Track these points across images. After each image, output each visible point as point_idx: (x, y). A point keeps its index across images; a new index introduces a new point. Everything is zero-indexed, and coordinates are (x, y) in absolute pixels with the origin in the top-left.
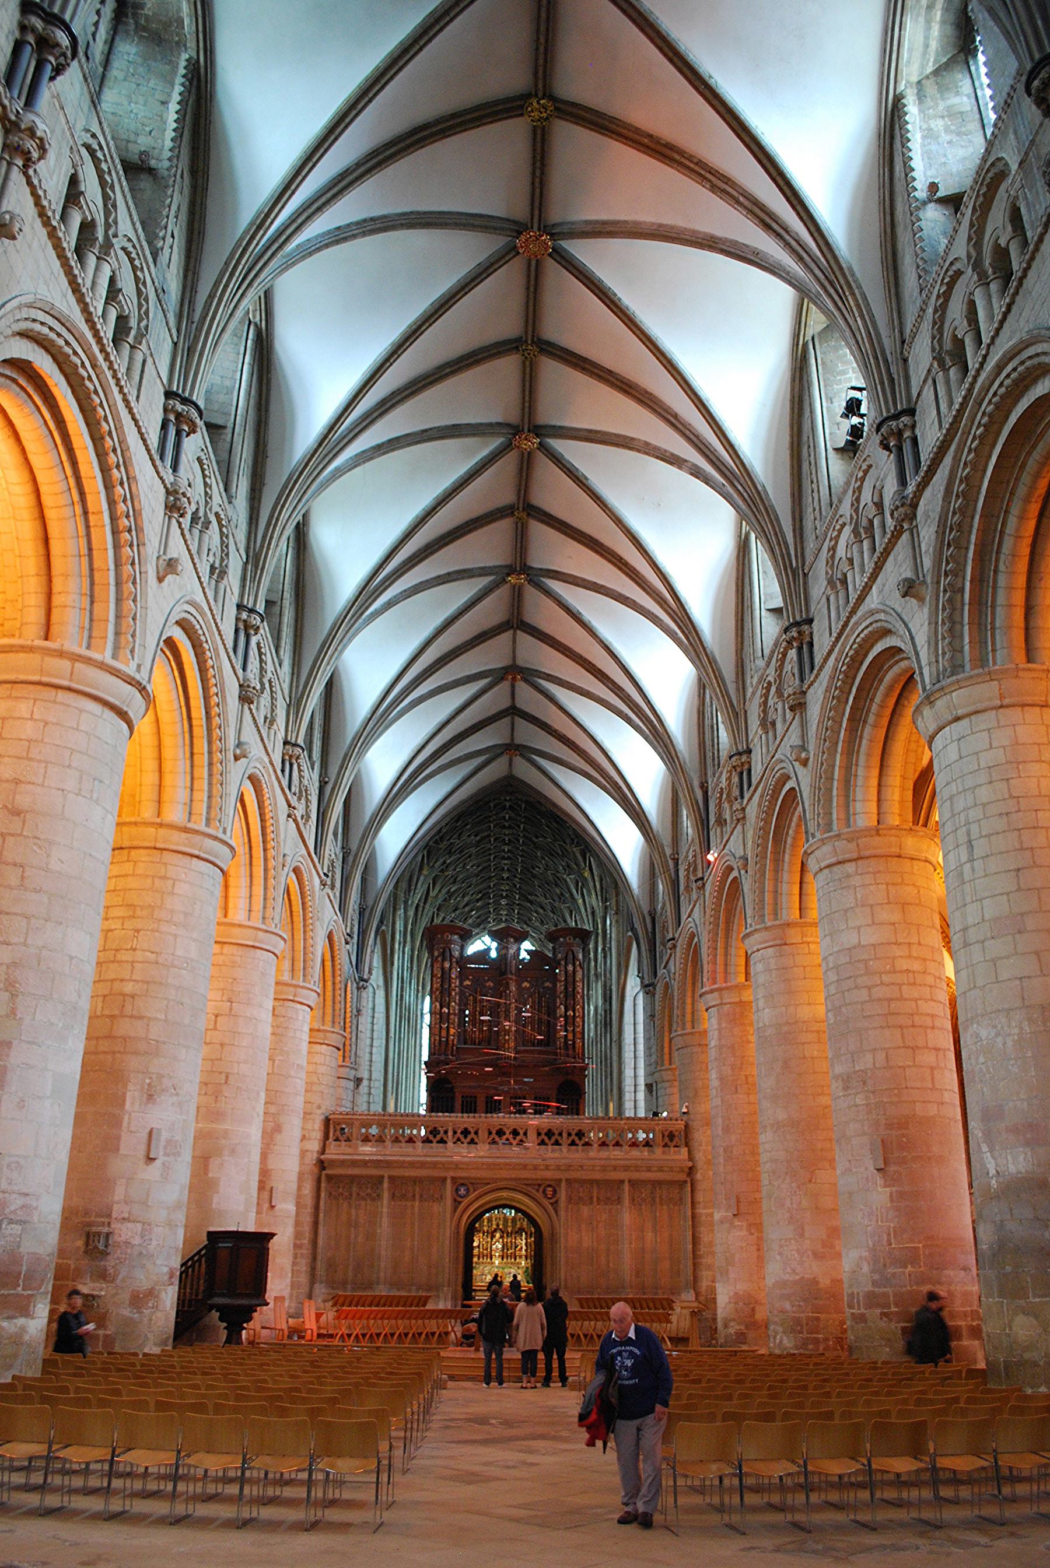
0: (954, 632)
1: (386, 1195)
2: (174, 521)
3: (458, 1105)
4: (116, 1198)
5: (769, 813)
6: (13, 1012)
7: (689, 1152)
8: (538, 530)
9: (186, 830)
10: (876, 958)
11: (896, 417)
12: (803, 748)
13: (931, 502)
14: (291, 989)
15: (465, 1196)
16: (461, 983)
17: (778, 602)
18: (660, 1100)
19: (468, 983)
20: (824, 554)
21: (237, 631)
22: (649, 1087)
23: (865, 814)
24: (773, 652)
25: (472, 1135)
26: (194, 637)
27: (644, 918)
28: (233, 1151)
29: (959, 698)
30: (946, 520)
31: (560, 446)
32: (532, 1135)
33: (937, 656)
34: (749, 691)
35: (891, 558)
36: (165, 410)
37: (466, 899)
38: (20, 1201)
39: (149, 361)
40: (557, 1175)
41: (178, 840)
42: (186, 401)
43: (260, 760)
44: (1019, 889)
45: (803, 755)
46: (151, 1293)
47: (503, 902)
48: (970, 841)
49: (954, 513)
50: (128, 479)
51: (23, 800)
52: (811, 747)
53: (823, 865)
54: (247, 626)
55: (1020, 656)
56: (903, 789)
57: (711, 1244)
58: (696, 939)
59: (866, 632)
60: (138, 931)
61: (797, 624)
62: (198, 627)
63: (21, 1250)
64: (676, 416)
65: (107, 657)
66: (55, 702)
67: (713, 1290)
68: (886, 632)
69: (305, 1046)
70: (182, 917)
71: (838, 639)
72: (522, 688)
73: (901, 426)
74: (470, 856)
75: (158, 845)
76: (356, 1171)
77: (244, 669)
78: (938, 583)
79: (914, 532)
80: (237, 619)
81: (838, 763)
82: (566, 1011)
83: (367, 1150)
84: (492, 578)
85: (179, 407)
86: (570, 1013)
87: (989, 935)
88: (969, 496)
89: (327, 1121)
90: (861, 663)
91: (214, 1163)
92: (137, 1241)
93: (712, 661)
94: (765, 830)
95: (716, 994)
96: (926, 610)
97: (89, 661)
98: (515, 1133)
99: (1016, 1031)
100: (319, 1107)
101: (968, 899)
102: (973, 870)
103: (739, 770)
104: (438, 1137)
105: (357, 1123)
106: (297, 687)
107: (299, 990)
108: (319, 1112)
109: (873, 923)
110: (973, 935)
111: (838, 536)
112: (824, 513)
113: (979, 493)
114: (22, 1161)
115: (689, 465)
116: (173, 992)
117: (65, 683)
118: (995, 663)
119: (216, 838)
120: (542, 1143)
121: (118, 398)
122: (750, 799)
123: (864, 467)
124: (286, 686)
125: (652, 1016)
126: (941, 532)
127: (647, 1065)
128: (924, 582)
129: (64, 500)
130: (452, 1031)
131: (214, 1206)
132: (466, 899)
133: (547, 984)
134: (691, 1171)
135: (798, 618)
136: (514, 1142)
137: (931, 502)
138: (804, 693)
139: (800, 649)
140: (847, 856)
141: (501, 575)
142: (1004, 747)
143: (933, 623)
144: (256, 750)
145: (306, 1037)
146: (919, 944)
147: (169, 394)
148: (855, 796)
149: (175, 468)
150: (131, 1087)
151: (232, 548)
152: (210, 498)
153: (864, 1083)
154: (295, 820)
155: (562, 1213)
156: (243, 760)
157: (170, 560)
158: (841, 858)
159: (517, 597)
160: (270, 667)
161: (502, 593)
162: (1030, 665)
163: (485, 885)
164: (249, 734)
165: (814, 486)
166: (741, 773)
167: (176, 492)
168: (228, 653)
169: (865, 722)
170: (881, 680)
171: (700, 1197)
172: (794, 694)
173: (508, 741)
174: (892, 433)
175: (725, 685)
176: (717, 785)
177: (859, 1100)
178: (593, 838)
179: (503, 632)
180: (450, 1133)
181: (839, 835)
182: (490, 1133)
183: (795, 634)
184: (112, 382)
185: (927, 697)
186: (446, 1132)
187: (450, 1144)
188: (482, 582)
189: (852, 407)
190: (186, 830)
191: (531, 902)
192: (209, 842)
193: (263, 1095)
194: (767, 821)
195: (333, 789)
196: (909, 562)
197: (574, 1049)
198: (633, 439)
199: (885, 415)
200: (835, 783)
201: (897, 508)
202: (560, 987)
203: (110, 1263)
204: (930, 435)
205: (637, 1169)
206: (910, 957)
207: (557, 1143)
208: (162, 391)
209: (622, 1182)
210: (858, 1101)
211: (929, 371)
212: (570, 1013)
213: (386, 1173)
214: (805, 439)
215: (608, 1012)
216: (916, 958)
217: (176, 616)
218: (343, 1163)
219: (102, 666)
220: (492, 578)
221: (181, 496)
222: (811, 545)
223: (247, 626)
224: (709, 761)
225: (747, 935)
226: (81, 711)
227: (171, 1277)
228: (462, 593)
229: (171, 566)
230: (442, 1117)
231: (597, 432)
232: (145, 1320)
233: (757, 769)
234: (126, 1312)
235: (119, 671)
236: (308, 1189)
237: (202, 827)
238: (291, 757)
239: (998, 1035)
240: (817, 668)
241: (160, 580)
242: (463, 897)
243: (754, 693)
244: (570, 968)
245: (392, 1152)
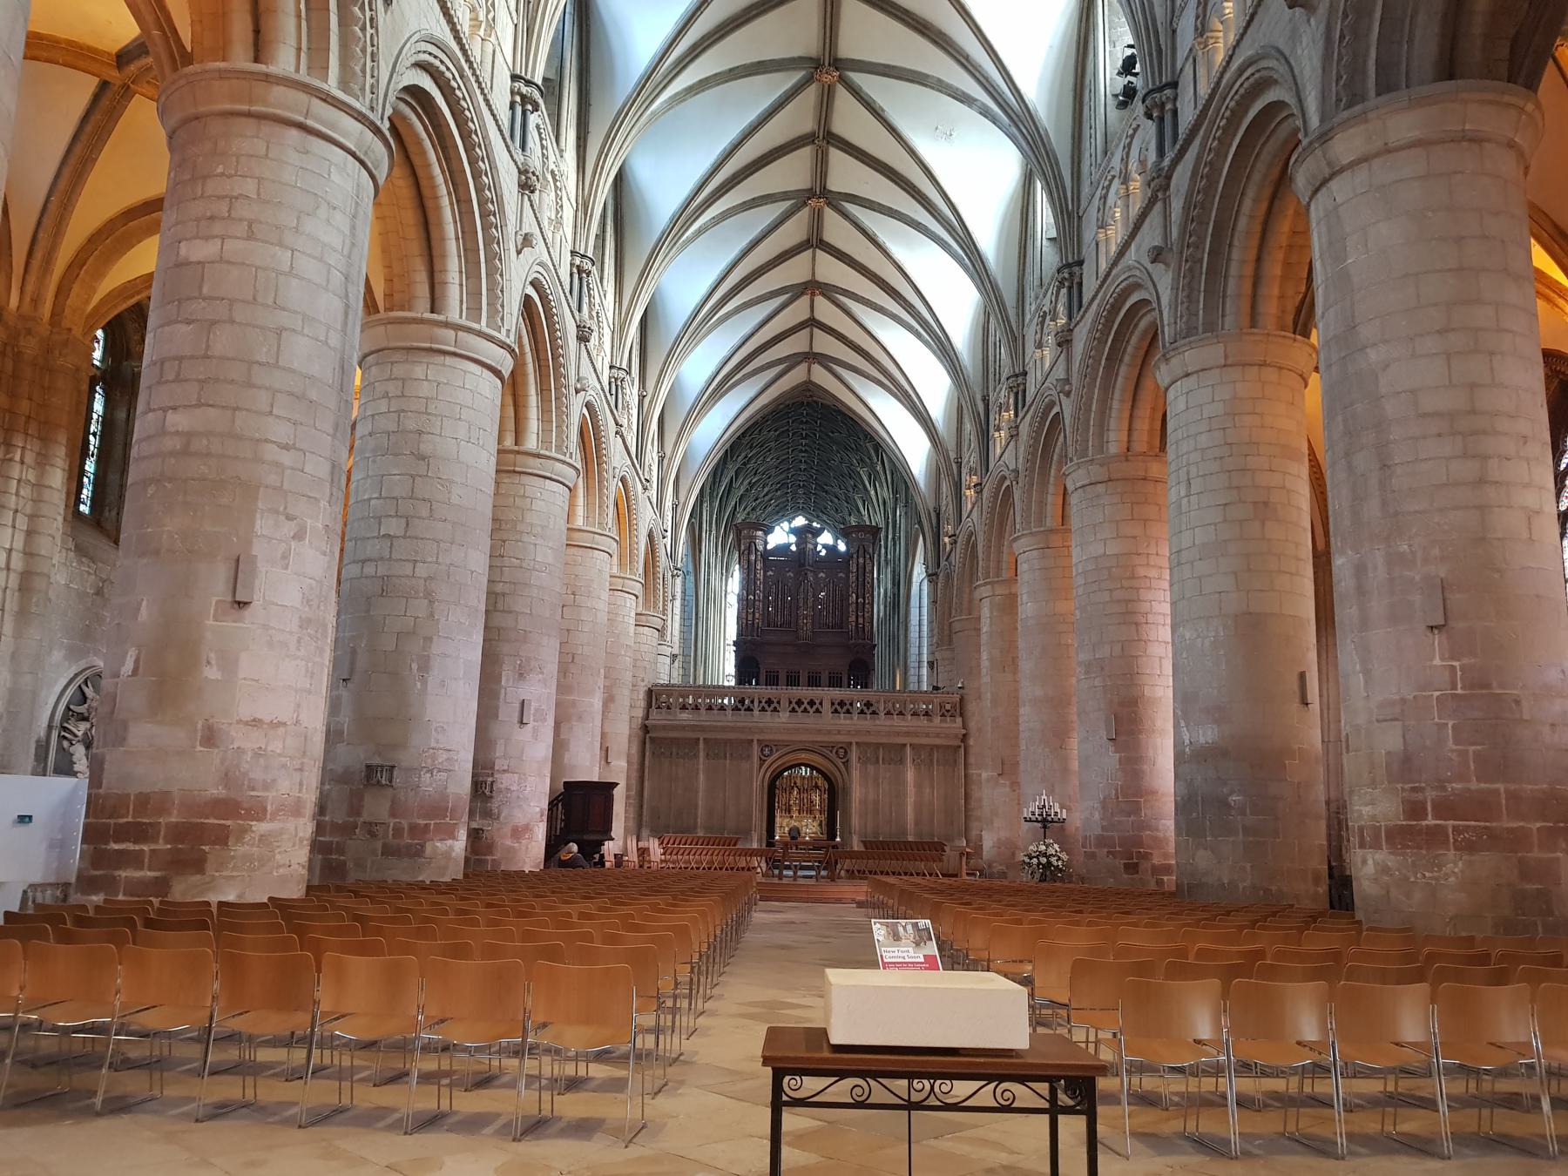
0: (1191, 299)
1: (702, 755)
2: (526, 198)
4: (497, 755)
5: (1038, 432)
6: (432, 615)
8: (836, 156)
9: (539, 456)
10: (1117, 566)
11: (1161, 89)
12: (1067, 381)
13: (1181, 177)
14: (620, 580)
16: (765, 575)
17: (1053, 234)
18: (940, 675)
19: (770, 573)
20: (1096, 201)
21: (571, 275)
22: (931, 664)
23: (1115, 441)
24: (1049, 284)
25: (775, 705)
26: (541, 291)
27: (929, 514)
28: (580, 718)
29: (1191, 357)
30: (1190, 202)
32: (827, 707)
33: (1176, 318)
34: (1027, 321)
35: (1147, 221)
36: (512, 93)
37: (766, 490)
38: (445, 756)
39: (498, 50)
40: (847, 739)
41: (534, 465)
42: (529, 83)
43: (594, 389)
44: (1225, 521)
45: (1067, 388)
46: (527, 828)
47: (801, 491)
48: (1189, 480)
49: (1199, 192)
50: (491, 169)
51: (425, 448)
52: (1075, 380)
53: (1078, 485)
54: (580, 270)
55: (1246, 320)
56: (1152, 419)
57: (980, 800)
58: (973, 538)
59: (1124, 284)
60: (504, 541)
61: (1068, 265)
62: (545, 283)
63: (448, 791)
64: (967, 58)
65: (483, 326)
66: (444, 365)
67: (980, 837)
68: (1137, 286)
69: (632, 628)
70: (539, 529)
71: (1101, 286)
72: (820, 301)
73: (1164, 98)
74: (769, 450)
75: (517, 469)
77: (580, 310)
78: (1181, 253)
79: (1166, 202)
80: (572, 265)
81: (1095, 397)
82: (857, 598)
84: (793, 201)
85: (524, 90)
86: (860, 600)
87: (1198, 557)
88: (1212, 178)
89: (650, 692)
90: (1120, 309)
91: (564, 727)
92: (514, 788)
93: (995, 287)
94: (1034, 446)
95: (989, 587)
96: (1170, 274)
97: (469, 330)
98: (812, 703)
99: (1213, 634)
100: (643, 680)
101: (1184, 527)
102: (1189, 501)
103: (1015, 390)
104: (746, 707)
105: (676, 694)
106: (620, 314)
107: (626, 581)
108: (643, 684)
110: (1185, 556)
111: (1109, 186)
112: (1099, 161)
113: (1220, 175)
114: (445, 727)
115: (978, 104)
116: (536, 591)
117: (452, 349)
118: (1222, 329)
119: (564, 462)
120: (836, 711)
121: (481, 98)
122: (1024, 418)
123: (1134, 126)
124: (610, 315)
125: (935, 602)
126: (1187, 208)
127: (930, 645)
128: (1171, 249)
130: (757, 615)
131: (566, 760)
132: (766, 490)
133: (841, 574)
134: (965, 738)
135: (1070, 260)
136: (811, 711)
137: (1181, 177)
138: (1072, 330)
139: (1070, 288)
140: (1099, 479)
141: (802, 198)
142: (1224, 401)
143: (1175, 289)
144: (593, 381)
145: (632, 622)
147: (515, 78)
148: (1108, 425)
149: (523, 147)
150: (505, 667)
151: (565, 199)
152: (547, 158)
153: (1102, 669)
154: (622, 436)
156: (583, 393)
157: (526, 234)
158: (1093, 480)
159: (817, 221)
160: (597, 300)
161: (805, 212)
162: (1254, 330)
163: (783, 476)
164: (586, 370)
165: (1093, 131)
166: (1017, 394)
167: (526, 171)
168: (566, 297)
169: (1121, 361)
170: (1136, 326)
171: (972, 760)
172: (1063, 331)
173: (807, 350)
174: (1155, 105)
175: (1005, 310)
176: (997, 400)
177: (1097, 682)
178: (884, 440)
179: (805, 250)
181: (1093, 460)
182: (790, 703)
183: (1066, 275)
184: (475, 85)
185: (1164, 355)
186: (752, 702)
187: (756, 712)
188: (785, 205)
189: (1128, 66)
190: (539, 456)
191: (826, 492)
192: (558, 465)
193: (602, 671)
194: (1037, 440)
195: (651, 402)
196: (1159, 231)
197: (865, 632)
198: (928, 76)
199: (1150, 86)
200: (1093, 414)
201: (1153, 179)
202: (852, 577)
203: (494, 805)
204: (1187, 115)
205: (916, 734)
207: (848, 712)
208: (508, 74)
209: (905, 745)
210: (1096, 684)
211: (1191, 50)
212: (860, 600)
214: (1087, 82)
215: (896, 595)
217: (530, 279)
218: (664, 727)
219: (480, 334)
220: (793, 201)
221: (530, 175)
222: (1086, 190)
223: (580, 270)
224: (991, 376)
225: (1015, 540)
226: (465, 372)
227: (542, 816)
228: (767, 214)
229: (527, 241)
231: (894, 67)
232: (524, 848)
233: (1031, 391)
234: (508, 842)
235: (493, 337)
236: (635, 750)
237: (553, 454)
238: (616, 379)
239: (1199, 636)
240: (1027, 404)
241: (519, 252)
242: (764, 487)
243: (1031, 320)
244: (861, 560)
245: (703, 717)
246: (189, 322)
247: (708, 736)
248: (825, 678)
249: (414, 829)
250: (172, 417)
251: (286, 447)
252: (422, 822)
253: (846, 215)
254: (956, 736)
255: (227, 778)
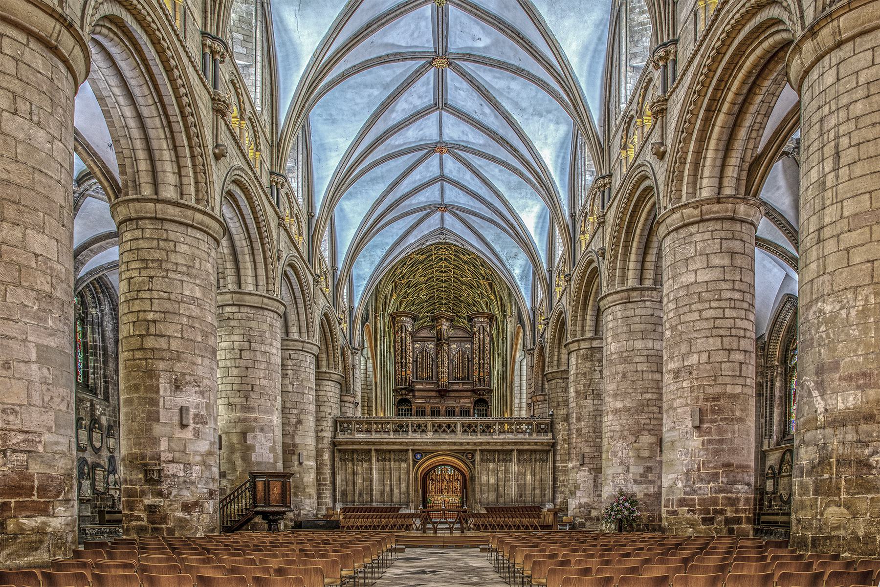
7: (553, 435)
10: (707, 291)
32: (459, 428)
76: (355, 447)
83: (360, 436)
98: (449, 426)
102: (837, 177)
109: (708, 267)
120: (465, 431)
134: (554, 445)
146: (741, 281)
182: (434, 426)
205: (522, 444)
206: (733, 289)
207: (474, 431)
213: (373, 448)
216: (738, 291)
218: (346, 443)
247: (378, 448)
253: (463, 74)
254: (548, 444)
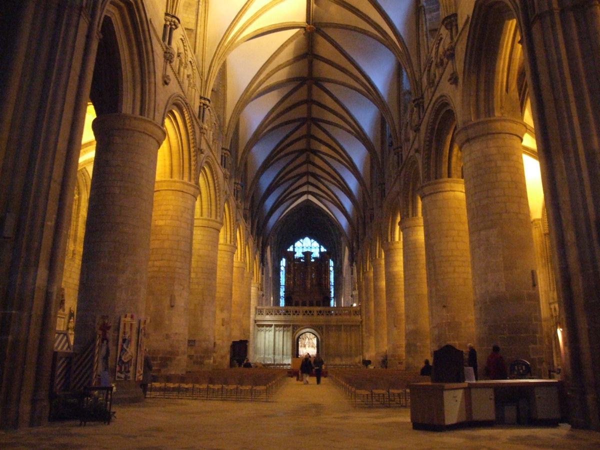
3: (294, 304)
15: (296, 330)
16: (294, 269)
31: (321, 123)
32: (315, 313)
36: (222, 153)
40: (323, 323)
98: (310, 312)
120: (318, 314)
129: (205, 186)
155: (324, 335)
161: (305, 155)
180: (292, 312)
219: (214, 221)
230: (289, 308)
234: (219, 360)
246: (159, 240)
247: (276, 323)
248: (315, 302)
249: (201, 357)
250: (155, 263)
251: (180, 268)
252: (202, 355)
255: (171, 346)
